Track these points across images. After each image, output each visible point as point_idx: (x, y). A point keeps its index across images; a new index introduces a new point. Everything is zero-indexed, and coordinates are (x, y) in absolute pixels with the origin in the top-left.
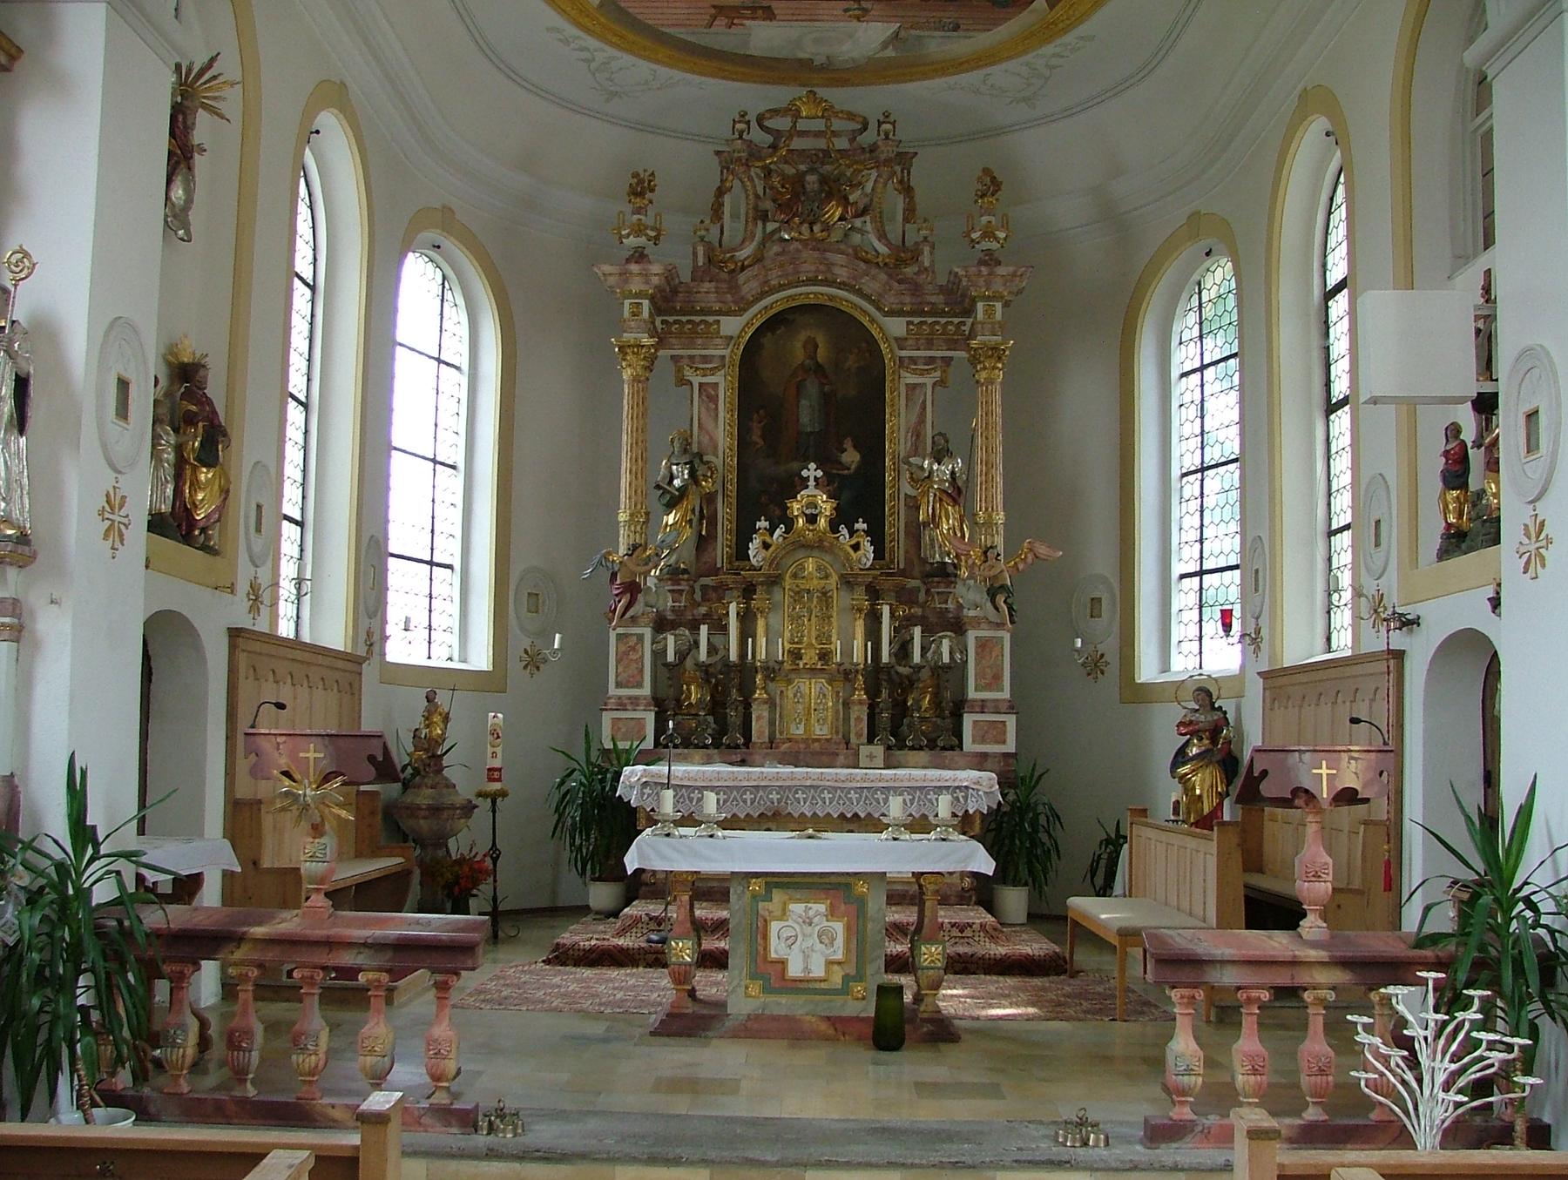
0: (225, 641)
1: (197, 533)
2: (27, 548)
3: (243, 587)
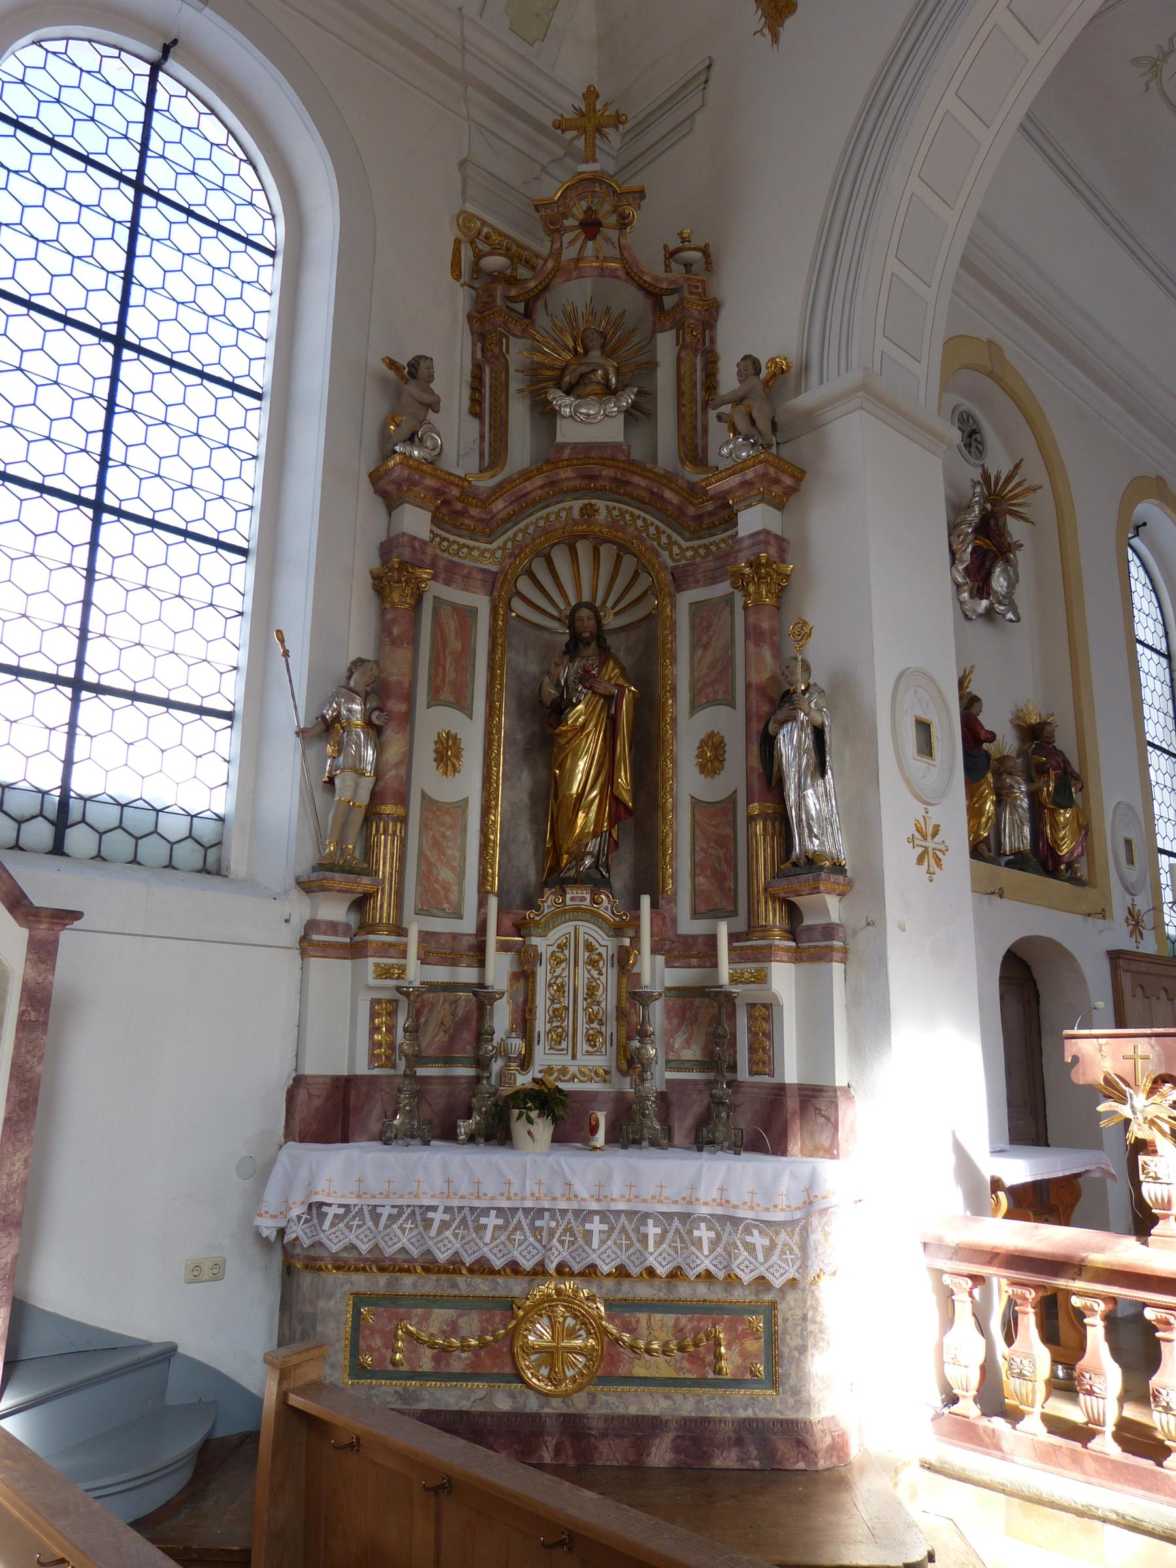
0: (1105, 965)
1: (1063, 867)
2: (841, 878)
3: (1119, 912)
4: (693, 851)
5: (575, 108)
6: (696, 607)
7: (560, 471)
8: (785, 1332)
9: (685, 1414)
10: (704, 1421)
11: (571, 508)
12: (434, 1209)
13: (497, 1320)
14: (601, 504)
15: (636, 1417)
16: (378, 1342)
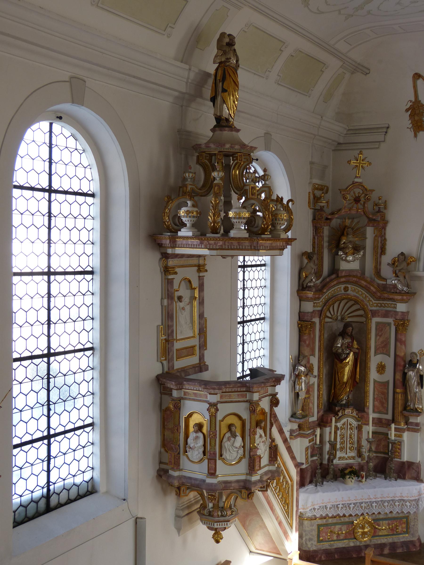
4: (374, 394)
5: (355, 157)
6: (377, 324)
7: (341, 279)
8: (411, 522)
9: (390, 542)
10: (394, 543)
11: (341, 287)
12: (339, 504)
13: (350, 526)
14: (349, 286)
15: (380, 544)
16: (324, 534)
